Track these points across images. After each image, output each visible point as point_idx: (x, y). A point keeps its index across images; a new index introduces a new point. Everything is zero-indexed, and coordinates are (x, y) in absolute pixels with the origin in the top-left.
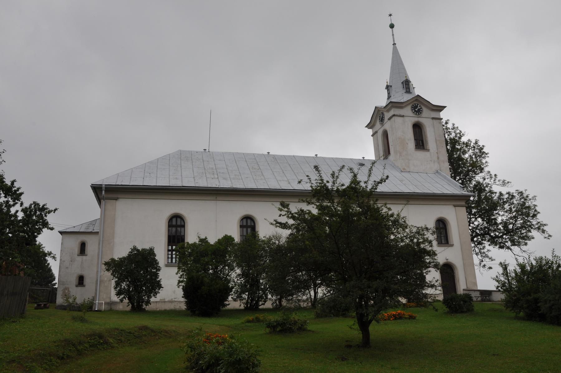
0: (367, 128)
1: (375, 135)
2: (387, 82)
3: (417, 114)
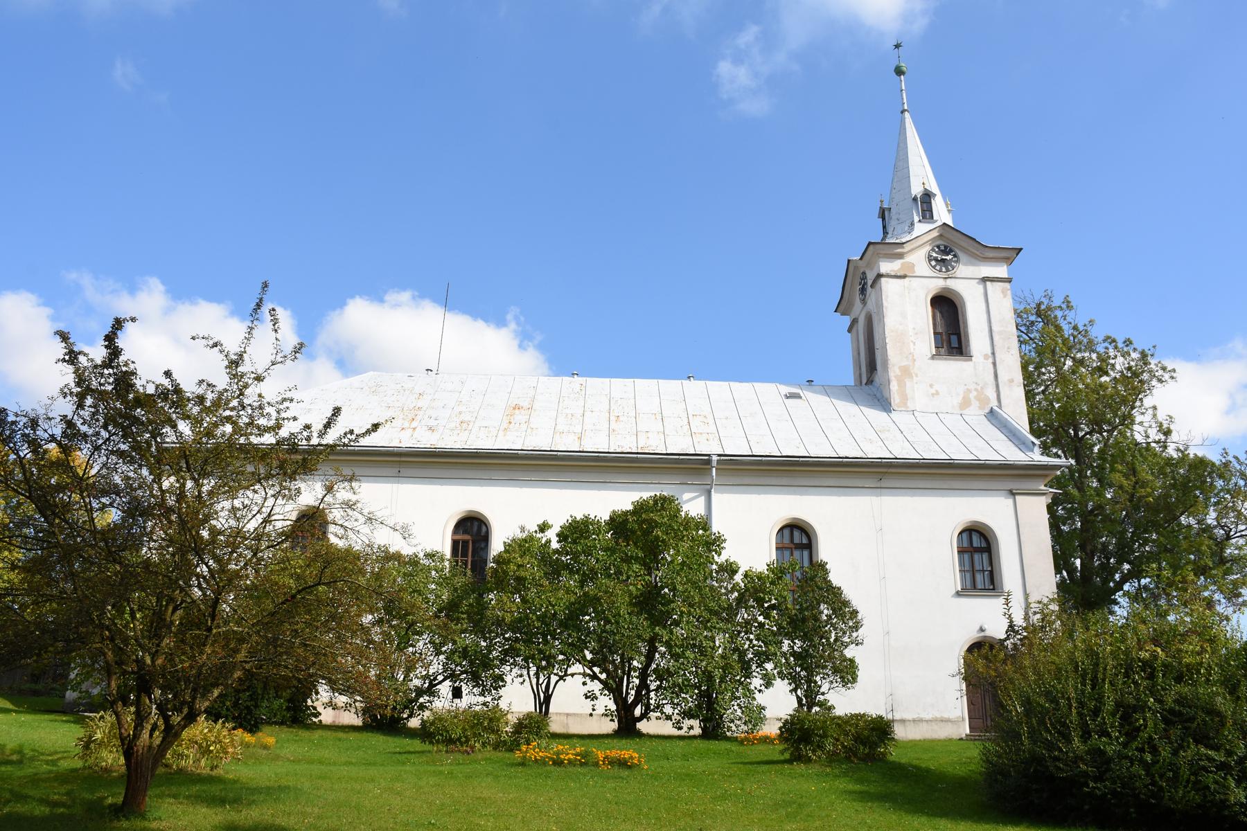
0: (838, 314)
1: (854, 330)
2: (882, 201)
3: (944, 269)
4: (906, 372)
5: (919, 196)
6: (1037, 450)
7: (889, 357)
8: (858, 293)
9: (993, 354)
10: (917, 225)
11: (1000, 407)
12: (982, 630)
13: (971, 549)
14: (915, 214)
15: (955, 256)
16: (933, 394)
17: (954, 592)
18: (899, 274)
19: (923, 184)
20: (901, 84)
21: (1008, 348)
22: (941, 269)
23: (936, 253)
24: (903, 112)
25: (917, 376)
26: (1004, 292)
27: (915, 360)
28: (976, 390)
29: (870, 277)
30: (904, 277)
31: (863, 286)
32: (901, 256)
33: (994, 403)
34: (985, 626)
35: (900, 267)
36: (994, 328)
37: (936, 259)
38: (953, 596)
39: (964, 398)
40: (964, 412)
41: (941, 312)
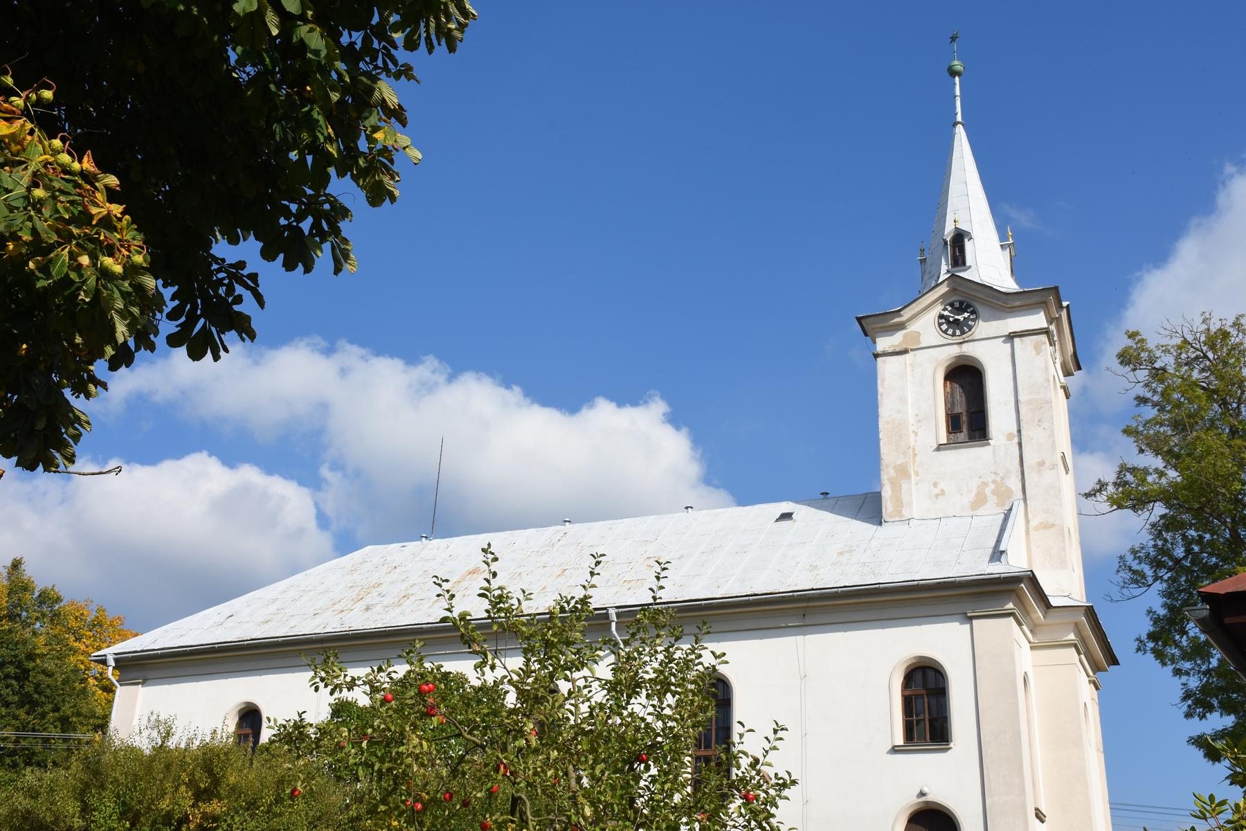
3: (958, 332)
5: (948, 239)
9: (1019, 431)
12: (922, 794)
16: (937, 496)
18: (898, 350)
21: (1040, 421)
23: (950, 312)
24: (955, 124)
25: (917, 474)
26: (1038, 349)
27: (915, 455)
28: (994, 482)
30: (905, 352)
32: (901, 326)
34: (926, 790)
37: (948, 322)
38: (888, 753)
39: (977, 495)
41: (962, 387)
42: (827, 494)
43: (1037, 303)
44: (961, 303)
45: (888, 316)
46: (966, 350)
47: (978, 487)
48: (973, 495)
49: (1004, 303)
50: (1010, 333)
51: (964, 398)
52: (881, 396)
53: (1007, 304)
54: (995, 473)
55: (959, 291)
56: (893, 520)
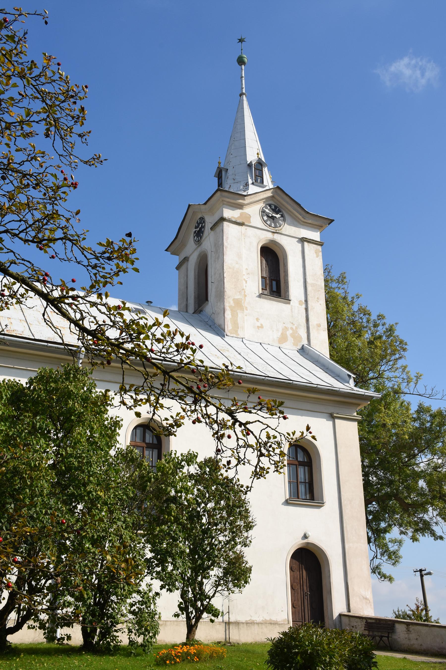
0: (169, 253)
1: (184, 268)
3: (273, 225)
4: (239, 304)
6: (352, 381)
7: (226, 289)
8: (193, 233)
9: (306, 301)
10: (251, 186)
11: (309, 343)
13: (296, 463)
14: (249, 178)
15: (282, 216)
16: (258, 327)
17: (284, 500)
19: (258, 154)
20: (242, 71)
21: (318, 298)
22: (271, 223)
23: (269, 210)
24: (241, 94)
27: (246, 296)
28: (292, 328)
29: (210, 221)
31: (201, 229)
32: (241, 207)
33: (305, 342)
34: (309, 533)
35: (239, 215)
36: (308, 280)
37: (268, 216)
38: (282, 504)
39: (282, 334)
40: (281, 346)
41: (266, 261)
42: (151, 302)
43: (318, 226)
44: (276, 207)
45: (237, 196)
46: (276, 238)
47: (283, 329)
48: (280, 334)
49: (303, 217)
50: (303, 238)
51: (268, 269)
52: (226, 248)
53: (304, 219)
54: (292, 323)
55: (275, 198)
56: (232, 335)
